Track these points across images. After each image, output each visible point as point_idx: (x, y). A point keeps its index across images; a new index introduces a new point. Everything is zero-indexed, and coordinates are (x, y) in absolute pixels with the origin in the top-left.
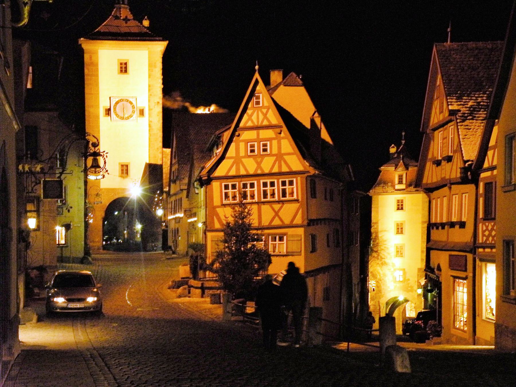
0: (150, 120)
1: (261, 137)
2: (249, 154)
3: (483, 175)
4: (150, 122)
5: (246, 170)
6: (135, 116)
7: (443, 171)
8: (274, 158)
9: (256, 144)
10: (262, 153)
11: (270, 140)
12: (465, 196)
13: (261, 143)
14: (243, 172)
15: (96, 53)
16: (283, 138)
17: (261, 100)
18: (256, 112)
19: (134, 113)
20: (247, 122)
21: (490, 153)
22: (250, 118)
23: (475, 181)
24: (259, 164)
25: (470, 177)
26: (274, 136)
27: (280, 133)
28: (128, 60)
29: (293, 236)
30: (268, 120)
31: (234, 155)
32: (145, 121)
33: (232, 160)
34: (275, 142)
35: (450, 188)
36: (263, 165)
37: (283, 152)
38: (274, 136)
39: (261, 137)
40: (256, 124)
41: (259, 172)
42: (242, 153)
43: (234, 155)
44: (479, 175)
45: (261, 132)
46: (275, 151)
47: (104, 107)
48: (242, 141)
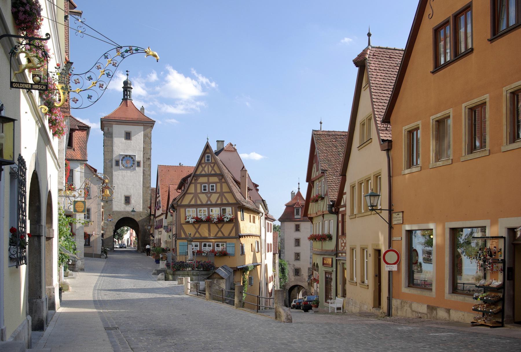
0: (144, 169)
1: (210, 181)
2: (203, 191)
4: (144, 170)
5: (201, 201)
6: (134, 166)
7: (319, 207)
8: (219, 194)
9: (207, 185)
10: (211, 191)
12: (332, 222)
13: (210, 185)
14: (199, 202)
15: (112, 127)
16: (224, 182)
17: (210, 158)
18: (207, 166)
19: (134, 164)
20: (202, 171)
22: (203, 170)
23: (337, 213)
25: (334, 211)
26: (218, 181)
27: (222, 179)
28: (131, 131)
30: (215, 171)
31: (193, 191)
32: (140, 170)
33: (192, 195)
34: (219, 185)
35: (323, 217)
37: (224, 191)
38: (218, 181)
39: (210, 181)
40: (207, 173)
41: (209, 203)
42: (199, 191)
43: (193, 191)
44: (339, 209)
46: (219, 190)
47: (115, 160)
48: (199, 183)
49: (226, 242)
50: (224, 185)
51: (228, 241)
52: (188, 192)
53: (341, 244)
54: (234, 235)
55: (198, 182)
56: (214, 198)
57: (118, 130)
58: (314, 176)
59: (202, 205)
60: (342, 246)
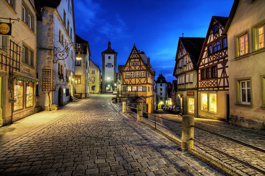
1: (136, 61)
3: (200, 68)
5: (132, 69)
11: (138, 62)
21: (203, 61)
24: (135, 68)
29: (144, 87)
31: (129, 65)
34: (139, 62)
36: (136, 68)
39: (136, 61)
42: (131, 65)
43: (129, 65)
44: (199, 68)
45: (136, 60)
46: (139, 64)
48: (131, 62)
49: (142, 86)
50: (141, 62)
51: (143, 85)
52: (127, 66)
53: (201, 84)
54: (146, 83)
55: (131, 61)
56: (137, 68)
57: (107, 56)
58: (179, 57)
59: (132, 71)
60: (201, 85)
